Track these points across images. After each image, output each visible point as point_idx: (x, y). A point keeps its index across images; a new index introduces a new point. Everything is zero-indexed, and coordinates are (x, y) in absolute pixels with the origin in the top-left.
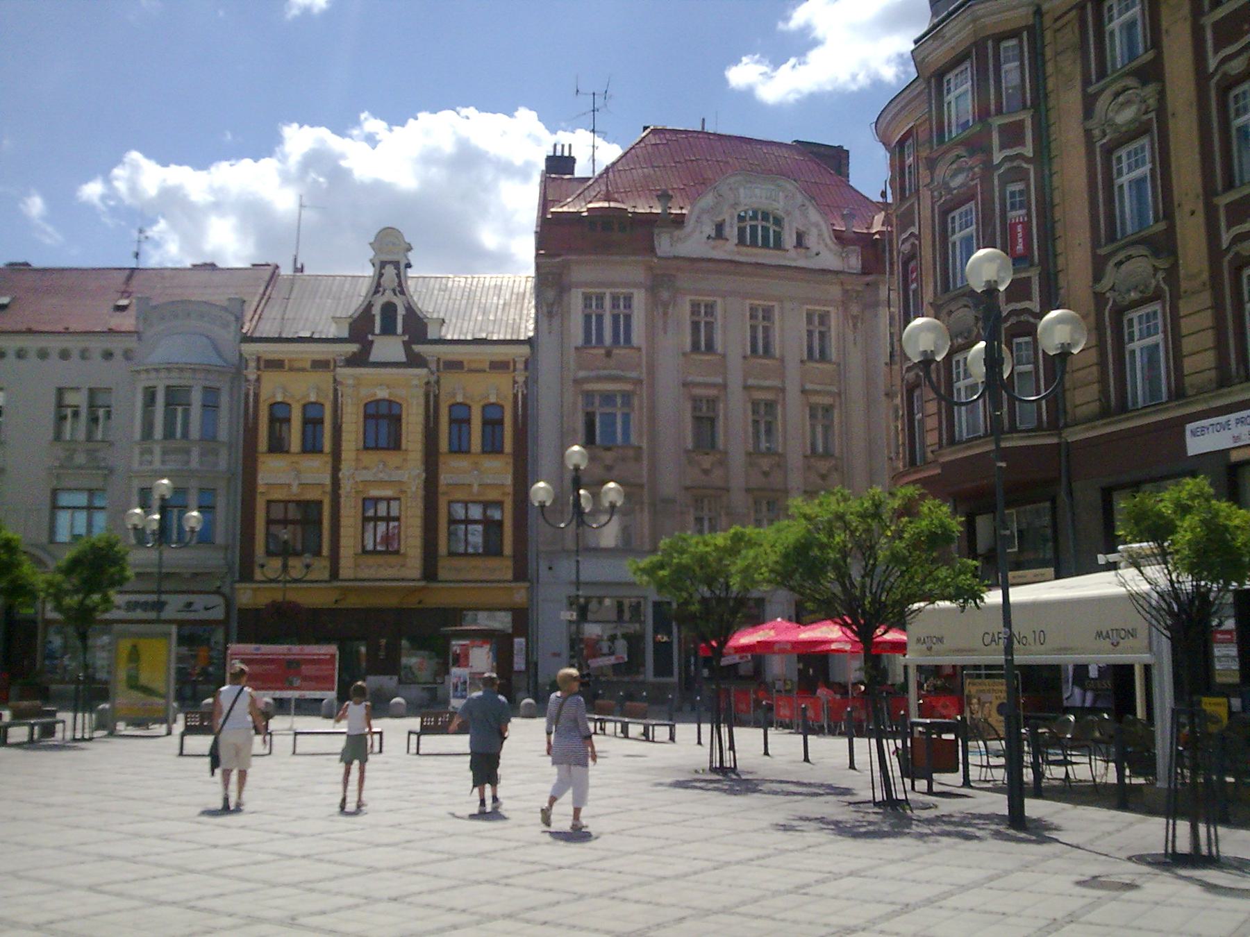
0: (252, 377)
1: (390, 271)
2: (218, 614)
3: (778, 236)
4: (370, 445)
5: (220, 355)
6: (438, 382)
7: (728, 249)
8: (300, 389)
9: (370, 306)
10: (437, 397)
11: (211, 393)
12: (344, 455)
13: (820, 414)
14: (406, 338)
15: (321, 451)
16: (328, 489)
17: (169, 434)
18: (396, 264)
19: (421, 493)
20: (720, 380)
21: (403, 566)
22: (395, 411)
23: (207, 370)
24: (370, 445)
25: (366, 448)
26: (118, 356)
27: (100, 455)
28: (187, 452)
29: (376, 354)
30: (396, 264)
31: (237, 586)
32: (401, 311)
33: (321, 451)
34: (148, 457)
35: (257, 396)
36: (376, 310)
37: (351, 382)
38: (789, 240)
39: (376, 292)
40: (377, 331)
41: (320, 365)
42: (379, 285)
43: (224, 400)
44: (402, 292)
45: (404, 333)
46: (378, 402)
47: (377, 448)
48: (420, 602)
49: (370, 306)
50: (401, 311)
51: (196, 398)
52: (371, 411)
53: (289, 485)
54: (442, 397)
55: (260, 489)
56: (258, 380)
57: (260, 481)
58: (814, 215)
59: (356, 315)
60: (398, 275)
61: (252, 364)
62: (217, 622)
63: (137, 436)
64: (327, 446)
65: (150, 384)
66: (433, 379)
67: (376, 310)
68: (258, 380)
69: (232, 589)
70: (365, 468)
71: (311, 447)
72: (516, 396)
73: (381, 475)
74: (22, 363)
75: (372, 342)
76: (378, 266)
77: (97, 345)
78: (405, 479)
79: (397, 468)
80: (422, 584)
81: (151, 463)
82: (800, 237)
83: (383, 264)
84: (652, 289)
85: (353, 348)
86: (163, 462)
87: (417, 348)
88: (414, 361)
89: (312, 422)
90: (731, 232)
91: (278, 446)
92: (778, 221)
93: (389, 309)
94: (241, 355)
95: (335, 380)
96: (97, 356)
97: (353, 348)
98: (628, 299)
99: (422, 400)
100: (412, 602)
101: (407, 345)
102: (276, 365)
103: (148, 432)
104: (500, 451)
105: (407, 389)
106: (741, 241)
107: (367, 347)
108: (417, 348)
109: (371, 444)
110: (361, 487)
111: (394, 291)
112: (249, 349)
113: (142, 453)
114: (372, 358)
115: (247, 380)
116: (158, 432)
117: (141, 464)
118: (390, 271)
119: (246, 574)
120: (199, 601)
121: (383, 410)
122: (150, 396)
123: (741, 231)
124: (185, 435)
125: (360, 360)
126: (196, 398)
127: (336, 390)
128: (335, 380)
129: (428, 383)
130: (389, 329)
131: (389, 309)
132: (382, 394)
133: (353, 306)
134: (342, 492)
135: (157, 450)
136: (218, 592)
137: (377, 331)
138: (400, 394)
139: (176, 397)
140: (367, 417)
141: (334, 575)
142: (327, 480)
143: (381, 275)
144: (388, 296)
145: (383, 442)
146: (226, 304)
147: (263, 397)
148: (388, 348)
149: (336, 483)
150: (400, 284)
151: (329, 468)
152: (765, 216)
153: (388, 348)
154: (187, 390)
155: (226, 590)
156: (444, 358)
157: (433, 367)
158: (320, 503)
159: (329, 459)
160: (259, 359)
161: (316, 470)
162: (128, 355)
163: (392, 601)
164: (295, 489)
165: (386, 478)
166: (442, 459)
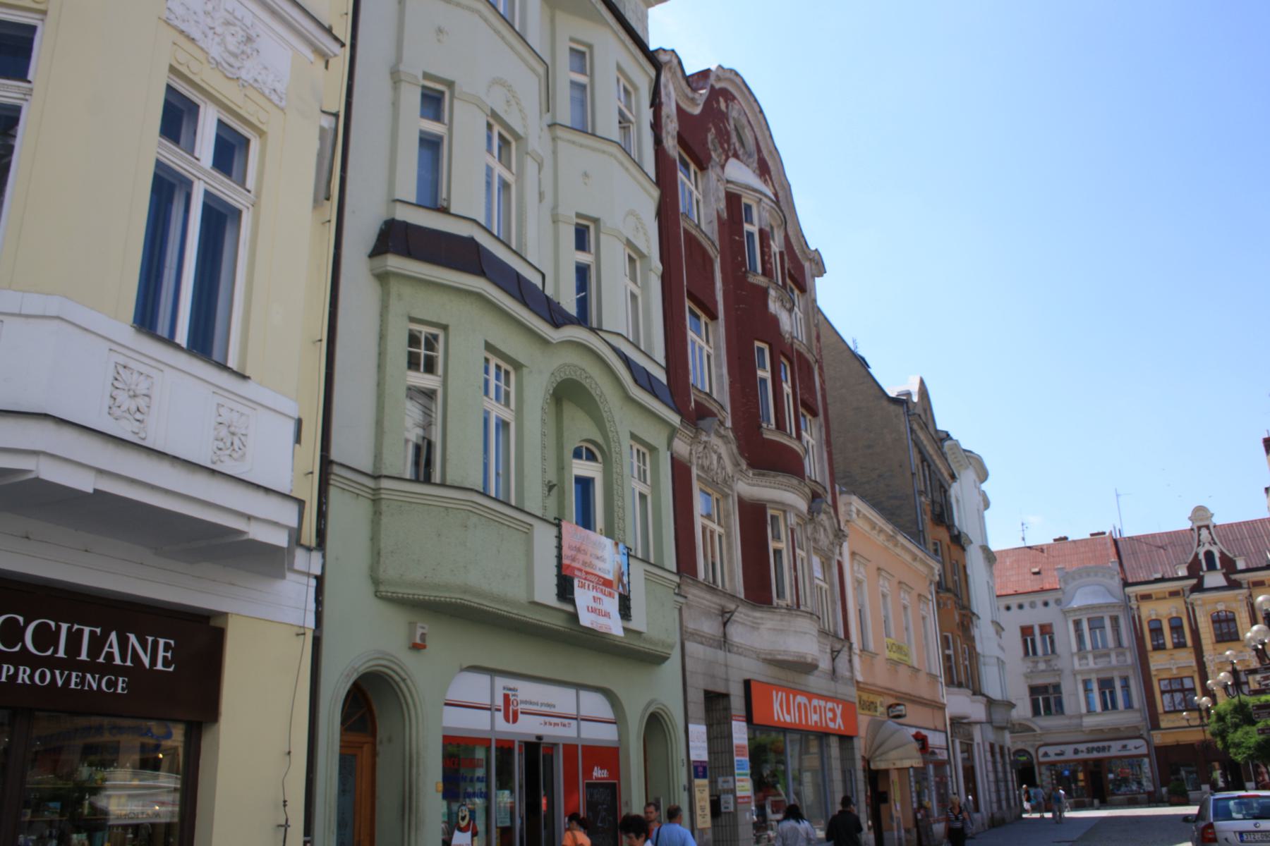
2: (1144, 750)
5: (1114, 596)
8: (1164, 610)
9: (1197, 555)
11: (1115, 620)
23: (1108, 606)
26: (1052, 604)
27: (1053, 663)
28: (1108, 655)
30: (1207, 527)
32: (1217, 555)
34: (1084, 661)
36: (1201, 556)
41: (1174, 594)
43: (1122, 622)
45: (1222, 566)
50: (1217, 555)
55: (1153, 673)
61: (1133, 599)
62: (1144, 756)
63: (1074, 648)
64: (1189, 642)
67: (1201, 556)
71: (1180, 645)
74: (1022, 612)
77: (1039, 599)
83: (1199, 528)
85: (1194, 581)
87: (1234, 577)
88: (1233, 585)
89: (1177, 628)
91: (1160, 647)
93: (1209, 555)
96: (1039, 604)
97: (1194, 581)
101: (1226, 576)
102: (1146, 597)
107: (1201, 579)
108: (1234, 577)
112: (1129, 590)
113: (1081, 659)
119: (1155, 725)
120: (1131, 744)
122: (1077, 624)
125: (1199, 588)
126: (1107, 623)
130: (1211, 567)
131: (1209, 555)
132: (1221, 607)
135: (1090, 657)
136: (1140, 737)
137: (1205, 567)
140: (1214, 622)
142: (1194, 664)
144: (1207, 547)
147: (1143, 617)
153: (1214, 579)
155: (1145, 735)
158: (1192, 677)
161: (1186, 658)
162: (1058, 602)
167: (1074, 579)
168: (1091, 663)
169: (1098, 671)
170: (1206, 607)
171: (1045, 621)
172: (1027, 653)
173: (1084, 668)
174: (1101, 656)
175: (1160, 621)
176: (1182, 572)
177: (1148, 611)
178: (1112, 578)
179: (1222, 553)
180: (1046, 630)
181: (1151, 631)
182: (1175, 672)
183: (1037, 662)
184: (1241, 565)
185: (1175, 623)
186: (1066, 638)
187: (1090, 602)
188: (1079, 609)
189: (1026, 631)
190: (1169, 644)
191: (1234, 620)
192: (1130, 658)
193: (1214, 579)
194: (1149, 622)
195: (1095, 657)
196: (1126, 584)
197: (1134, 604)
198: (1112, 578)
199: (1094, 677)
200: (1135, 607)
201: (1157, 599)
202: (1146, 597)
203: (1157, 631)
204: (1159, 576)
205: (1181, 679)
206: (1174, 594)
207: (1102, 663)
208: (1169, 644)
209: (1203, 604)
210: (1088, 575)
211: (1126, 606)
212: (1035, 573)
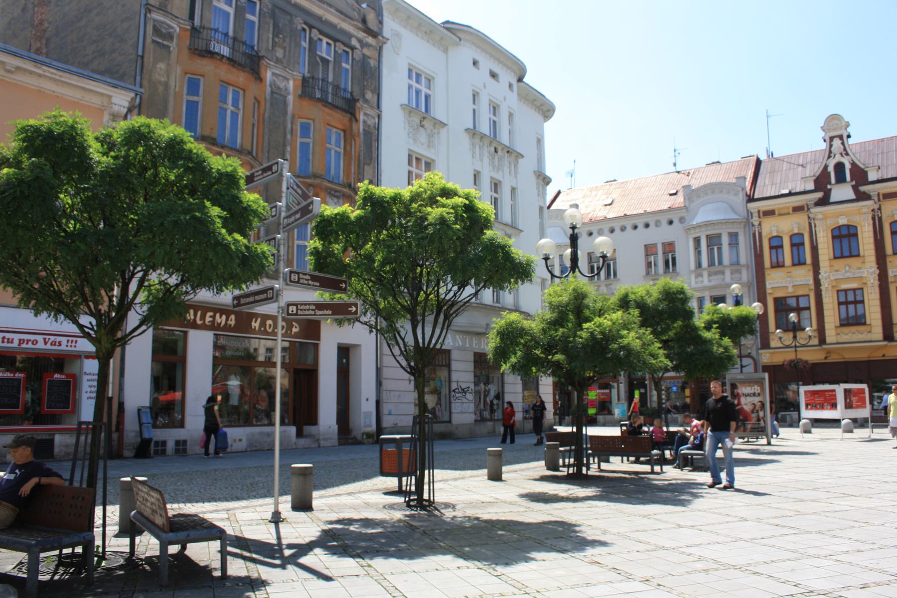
0: (756, 223)
1: (837, 143)
4: (839, 255)
5: (736, 213)
6: (880, 209)
8: (785, 226)
9: (826, 167)
10: (880, 219)
11: (734, 236)
12: (822, 264)
14: (854, 183)
15: (805, 264)
16: (812, 287)
17: (711, 263)
18: (841, 137)
19: (877, 283)
21: (870, 332)
22: (852, 231)
24: (839, 255)
25: (835, 258)
26: (676, 221)
28: (723, 273)
29: (834, 197)
30: (841, 137)
31: (760, 351)
32: (848, 166)
33: (805, 264)
34: (700, 279)
35: (760, 234)
36: (831, 169)
37: (820, 216)
39: (829, 157)
40: (833, 180)
41: (797, 209)
42: (830, 152)
43: (741, 239)
44: (847, 154)
45: (852, 180)
46: (839, 227)
47: (842, 257)
48: (884, 356)
49: (826, 167)
50: (848, 166)
51: (725, 240)
52: (837, 233)
53: (786, 287)
54: (884, 218)
55: (768, 291)
56: (760, 224)
57: (768, 286)
59: (817, 174)
60: (843, 144)
61: (755, 215)
63: (693, 266)
64: (809, 260)
65: (696, 235)
66: (876, 207)
67: (831, 169)
68: (760, 224)
69: (758, 353)
70: (837, 271)
71: (798, 262)
73: (848, 274)
75: (830, 190)
76: (828, 140)
78: (865, 275)
79: (859, 268)
80: (885, 343)
81: (702, 282)
83: (832, 139)
85: (819, 195)
86: (709, 281)
87: (863, 189)
88: (862, 197)
89: (797, 245)
91: (778, 265)
93: (840, 167)
94: (748, 211)
95: (809, 218)
96: (664, 223)
97: (819, 195)
99: (871, 222)
100: (877, 356)
101: (855, 188)
102: (770, 213)
103: (699, 265)
105: (860, 217)
107: (828, 193)
108: (863, 189)
109: (838, 254)
110: (834, 284)
111: (841, 154)
112: (753, 206)
113: (696, 277)
114: (832, 199)
115: (753, 225)
116: (705, 263)
117: (696, 283)
118: (837, 143)
121: (844, 232)
122: (697, 241)
124: (720, 263)
125: (824, 201)
126: (725, 240)
127: (810, 224)
128: (809, 218)
129: (873, 210)
130: (841, 179)
131: (840, 167)
132: (843, 221)
133: (817, 170)
134: (823, 288)
135: (705, 274)
137: (833, 180)
138: (855, 220)
139: (714, 241)
140: (834, 237)
141: (822, 341)
143: (831, 146)
144: (838, 158)
145: (846, 253)
146: (734, 181)
147: (764, 234)
148: (842, 192)
149: (817, 283)
150: (845, 149)
151: (811, 273)
154: (719, 236)
155: (754, 354)
156: (883, 191)
157: (876, 199)
159: (810, 268)
160: (759, 212)
161: (803, 276)
162: (682, 220)
163: (863, 356)
164: (790, 290)
165: (852, 276)
166: (888, 259)
167: (699, 197)
168: (705, 281)
169: (710, 288)
170: (826, 221)
171: (668, 239)
172: (648, 273)
173: (699, 285)
174: (716, 273)
175: (781, 237)
176: (811, 186)
177: (770, 227)
178: (736, 194)
179: (854, 165)
180: (669, 247)
181: (793, 245)
182: (790, 290)
183: (599, 286)
184: (872, 176)
185: (796, 240)
186: (686, 255)
187: (722, 218)
188: (699, 226)
189: (649, 250)
190: (788, 261)
191: (856, 235)
192: (746, 275)
193: (842, 192)
194: (770, 239)
195: (709, 275)
196: (751, 199)
197: (755, 220)
198: (736, 194)
199: (707, 295)
200: (756, 223)
201: (780, 215)
202: (770, 213)
203: (777, 247)
204: (786, 191)
205: (797, 297)
206: (797, 209)
207: (716, 280)
208: (788, 261)
209: (825, 218)
210: (713, 192)
211: (747, 222)
212: (671, 195)
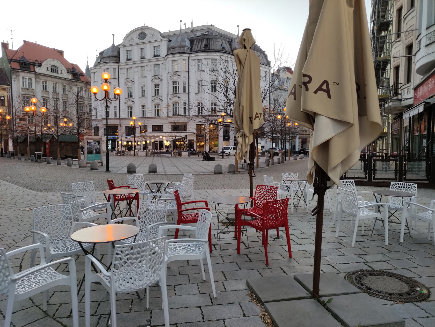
3: (57, 71)
7: (49, 73)
13: (65, 103)
20: (48, 96)
38: (59, 72)
58: (64, 68)
72: (8, 95)
82: (61, 71)
84: (35, 78)
90: (49, 69)
92: (57, 68)
98: (31, 79)
104: (4, 105)
106: (51, 71)
123: (51, 69)
152: (55, 66)
